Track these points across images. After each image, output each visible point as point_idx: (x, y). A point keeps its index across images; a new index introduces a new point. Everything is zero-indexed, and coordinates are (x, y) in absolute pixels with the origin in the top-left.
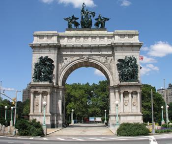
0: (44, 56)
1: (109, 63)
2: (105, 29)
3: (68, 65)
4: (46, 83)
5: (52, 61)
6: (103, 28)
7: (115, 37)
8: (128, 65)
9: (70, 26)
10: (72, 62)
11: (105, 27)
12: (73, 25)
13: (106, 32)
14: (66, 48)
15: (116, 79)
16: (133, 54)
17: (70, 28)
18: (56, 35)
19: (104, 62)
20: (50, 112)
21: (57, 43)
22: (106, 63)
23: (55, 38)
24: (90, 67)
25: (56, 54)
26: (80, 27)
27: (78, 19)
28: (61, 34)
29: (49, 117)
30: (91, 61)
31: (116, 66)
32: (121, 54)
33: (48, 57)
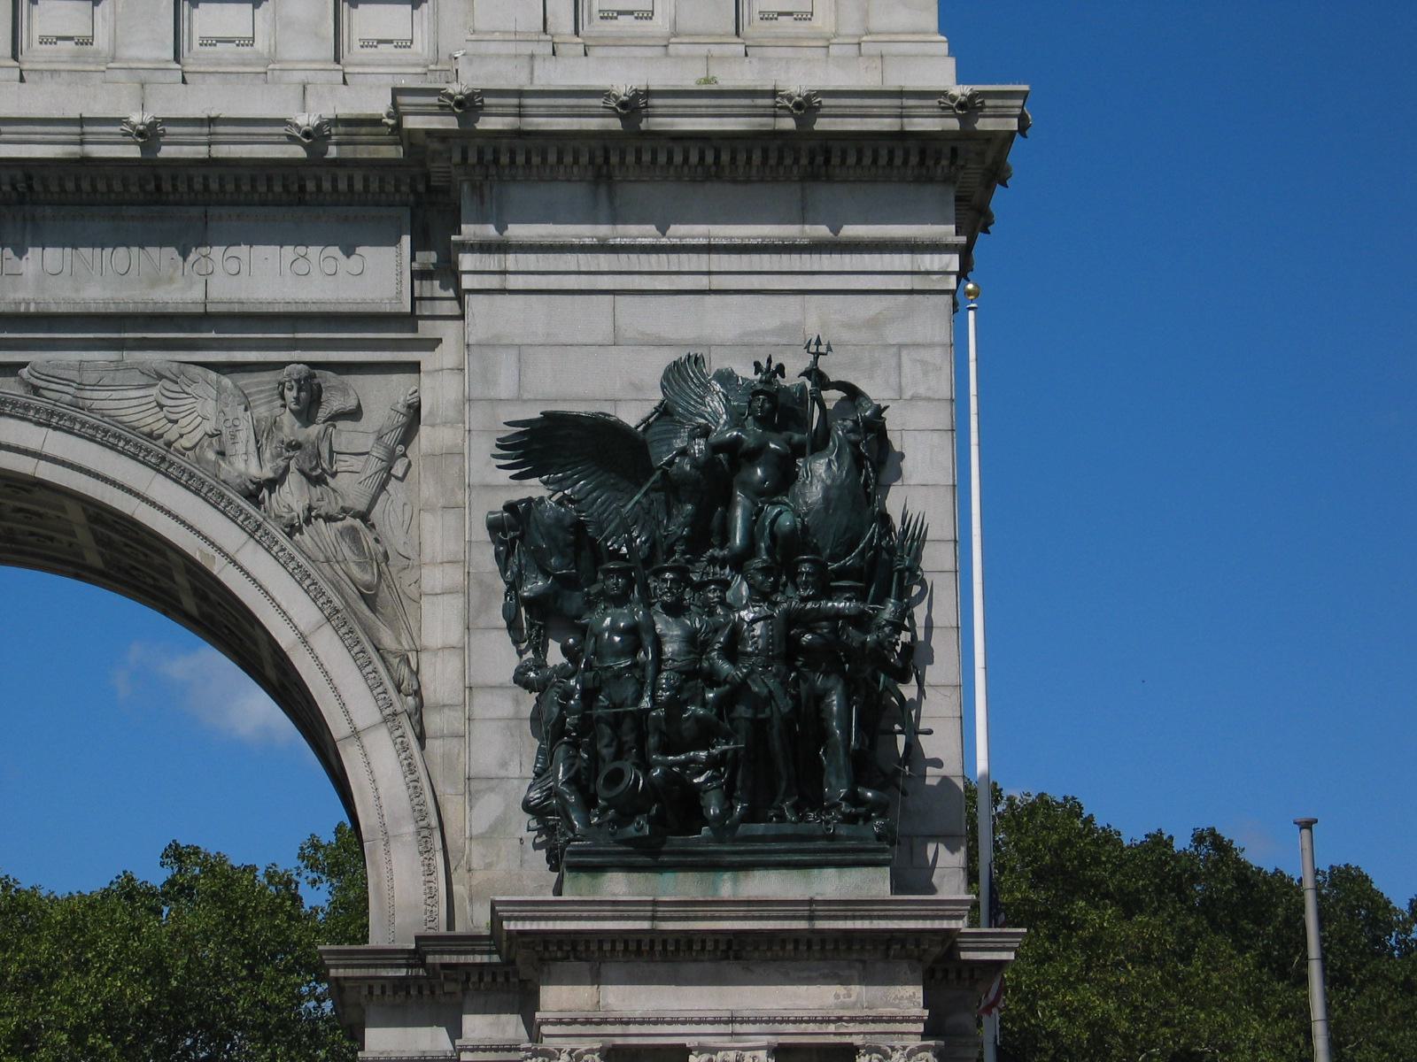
1: (351, 485)
8: (706, 532)
15: (491, 807)
16: (815, 317)
19: (247, 465)
22: (292, 496)
31: (485, 558)
32: (591, 318)
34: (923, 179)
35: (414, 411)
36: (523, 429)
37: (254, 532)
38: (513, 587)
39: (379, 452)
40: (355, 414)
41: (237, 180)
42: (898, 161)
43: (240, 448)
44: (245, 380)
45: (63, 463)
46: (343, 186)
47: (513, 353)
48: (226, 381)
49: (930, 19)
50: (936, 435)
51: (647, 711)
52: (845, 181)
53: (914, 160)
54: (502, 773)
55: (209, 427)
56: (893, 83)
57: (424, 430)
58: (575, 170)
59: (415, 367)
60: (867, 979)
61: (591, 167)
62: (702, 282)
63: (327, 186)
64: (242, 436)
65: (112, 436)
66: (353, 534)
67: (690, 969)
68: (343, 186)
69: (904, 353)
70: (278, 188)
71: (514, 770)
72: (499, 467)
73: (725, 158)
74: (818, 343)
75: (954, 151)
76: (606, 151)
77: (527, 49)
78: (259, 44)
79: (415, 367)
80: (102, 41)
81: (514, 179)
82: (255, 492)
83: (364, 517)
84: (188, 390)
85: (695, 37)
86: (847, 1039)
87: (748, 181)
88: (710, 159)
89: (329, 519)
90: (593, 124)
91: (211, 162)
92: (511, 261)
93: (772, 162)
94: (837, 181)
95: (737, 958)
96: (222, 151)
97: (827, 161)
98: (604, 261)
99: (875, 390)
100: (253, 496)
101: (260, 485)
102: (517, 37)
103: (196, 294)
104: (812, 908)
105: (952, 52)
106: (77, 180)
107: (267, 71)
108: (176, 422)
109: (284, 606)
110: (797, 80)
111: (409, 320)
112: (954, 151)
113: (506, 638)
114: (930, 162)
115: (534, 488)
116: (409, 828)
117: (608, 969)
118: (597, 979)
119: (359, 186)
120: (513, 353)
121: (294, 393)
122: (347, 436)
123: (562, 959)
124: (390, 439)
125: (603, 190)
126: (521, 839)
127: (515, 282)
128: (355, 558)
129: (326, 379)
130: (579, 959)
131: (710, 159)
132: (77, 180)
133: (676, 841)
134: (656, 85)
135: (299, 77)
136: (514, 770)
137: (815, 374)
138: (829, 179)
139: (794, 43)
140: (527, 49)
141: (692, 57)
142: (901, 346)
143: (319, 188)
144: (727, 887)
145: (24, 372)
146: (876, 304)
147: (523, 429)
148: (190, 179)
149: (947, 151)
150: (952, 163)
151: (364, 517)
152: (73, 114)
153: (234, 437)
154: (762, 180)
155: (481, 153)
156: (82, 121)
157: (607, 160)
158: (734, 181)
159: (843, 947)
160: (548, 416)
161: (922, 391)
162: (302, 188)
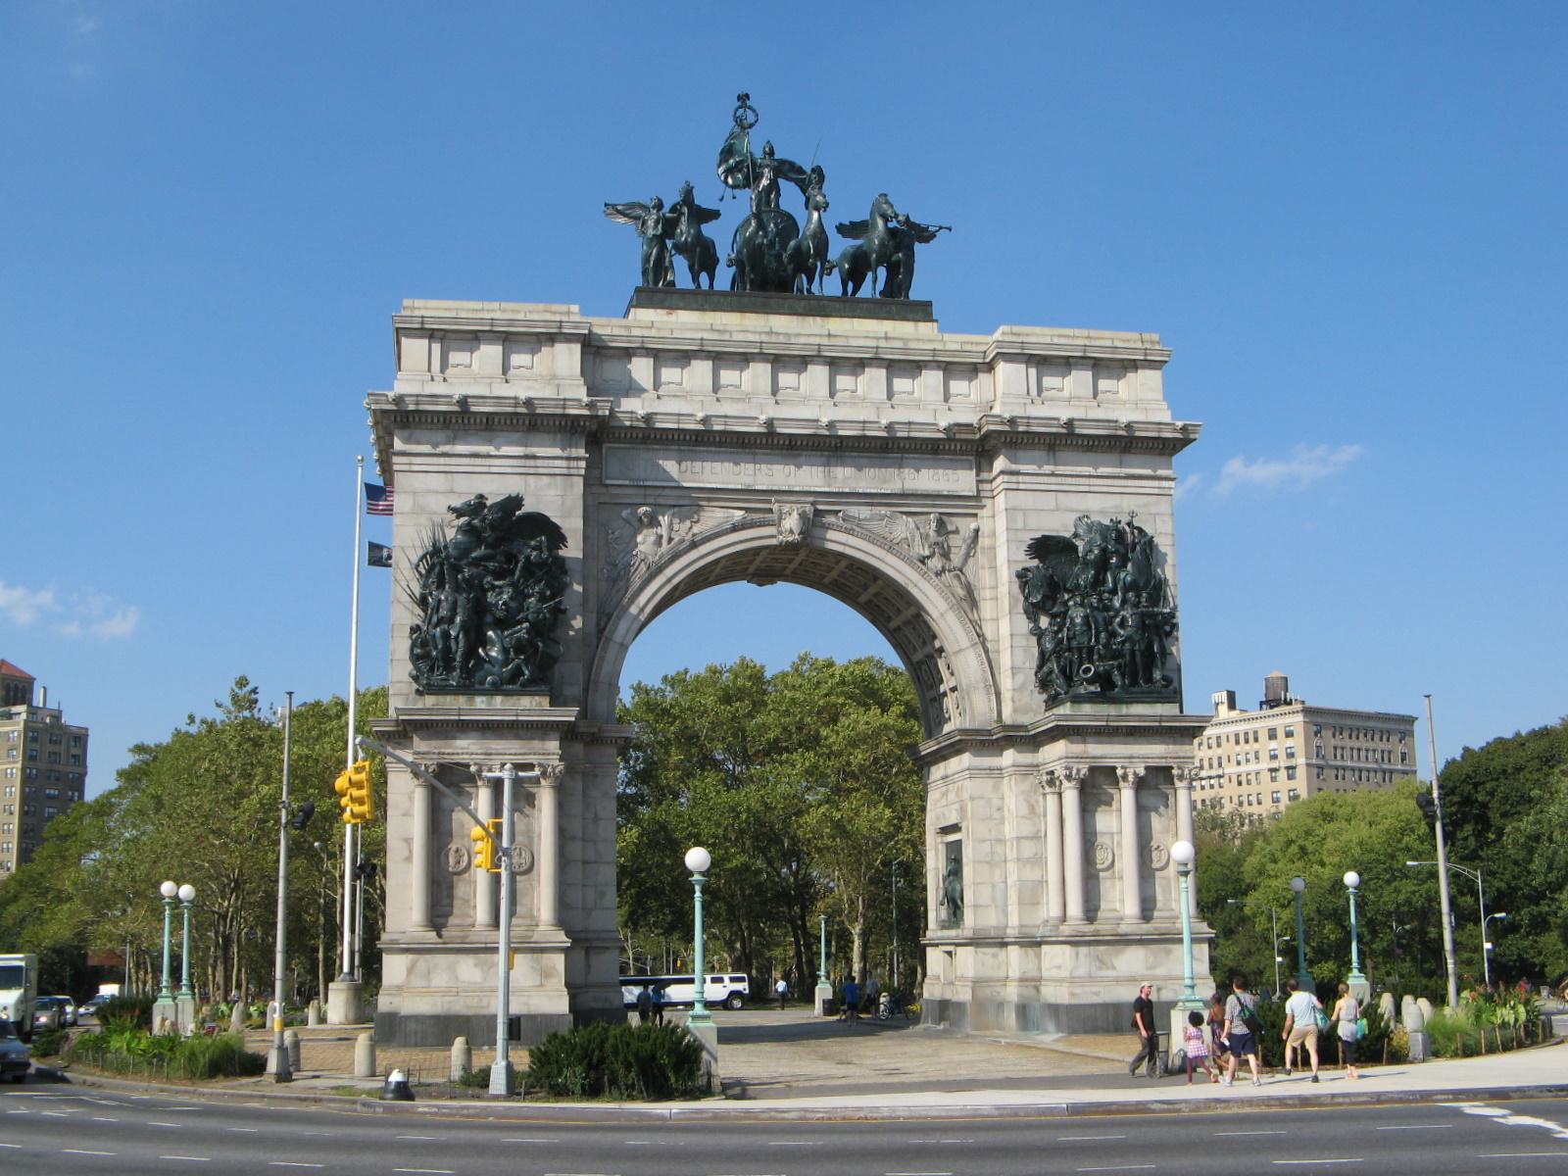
0: (495, 490)
1: (956, 559)
2: (922, 311)
3: (660, 569)
4: (526, 701)
5: (556, 536)
6: (897, 301)
7: (1002, 368)
9: (657, 269)
10: (694, 545)
11: (915, 294)
12: (681, 273)
13: (926, 329)
14: (651, 437)
17: (656, 290)
18: (569, 338)
20: (562, 921)
21: (582, 394)
22: (936, 563)
23: (567, 359)
24: (780, 585)
25: (579, 483)
26: (724, 277)
27: (714, 215)
28: (606, 328)
29: (559, 961)
30: (837, 540)
33: (515, 502)
35: (977, 531)
37: (923, 575)
38: (1026, 599)
39: (964, 547)
40: (957, 532)
43: (916, 543)
44: (918, 519)
45: (854, 548)
47: (1021, 513)
48: (910, 519)
49: (1160, 396)
51: (1093, 647)
55: (903, 536)
56: (1157, 420)
57: (980, 539)
59: (976, 515)
60: (1175, 743)
62: (1087, 489)
65: (873, 538)
66: (958, 576)
67: (1116, 739)
71: (1027, 665)
77: (1023, 401)
78: (916, 395)
79: (976, 515)
80: (860, 392)
82: (923, 560)
83: (961, 570)
85: (1079, 398)
89: (950, 571)
90: (1054, 430)
91: (909, 438)
92: (1021, 478)
96: (913, 434)
98: (1053, 480)
99: (1149, 530)
100: (923, 562)
101: (924, 558)
102: (1019, 396)
104: (1161, 718)
105: (1169, 408)
107: (918, 405)
110: (1124, 417)
111: (978, 497)
113: (1025, 617)
115: (1035, 562)
117: (1089, 739)
118: (1084, 742)
120: (1021, 513)
122: (954, 540)
124: (969, 541)
125: (1051, 454)
127: (1022, 486)
129: (945, 518)
133: (1107, 693)
134: (1076, 416)
135: (933, 407)
136: (1027, 665)
137: (1129, 524)
138: (1129, 452)
139: (1114, 402)
140: (1023, 401)
141: (1079, 406)
144: (1124, 710)
145: (841, 514)
151: (961, 570)
152: (861, 419)
156: (864, 422)
160: (1044, 537)
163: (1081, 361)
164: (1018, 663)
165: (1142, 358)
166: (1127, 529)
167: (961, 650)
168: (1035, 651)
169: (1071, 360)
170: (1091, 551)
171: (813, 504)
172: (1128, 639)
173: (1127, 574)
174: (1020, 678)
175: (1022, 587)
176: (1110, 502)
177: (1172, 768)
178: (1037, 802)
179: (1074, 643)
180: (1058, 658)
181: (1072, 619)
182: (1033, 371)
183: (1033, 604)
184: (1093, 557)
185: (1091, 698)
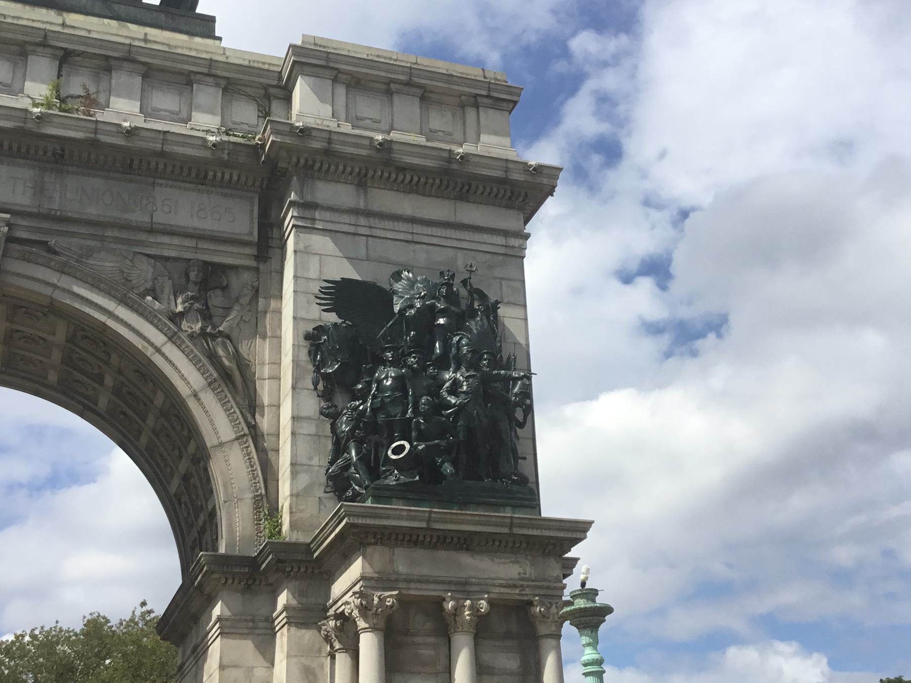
34: (508, 207)
36: (332, 285)
37: (172, 338)
38: (317, 369)
41: (174, 166)
42: (500, 196)
46: (227, 177)
47: (317, 258)
50: (519, 320)
51: (411, 419)
52: (474, 202)
53: (509, 194)
54: (309, 463)
55: (149, 285)
58: (350, 177)
61: (357, 178)
63: (219, 175)
64: (167, 290)
68: (227, 177)
69: (503, 282)
70: (193, 175)
71: (315, 461)
72: (317, 304)
73: (423, 180)
74: (471, 266)
75: (526, 194)
76: (367, 170)
81: (319, 179)
84: (137, 266)
86: (525, 598)
87: (429, 196)
88: (416, 179)
93: (443, 187)
94: (471, 202)
95: (467, 549)
97: (468, 191)
103: (147, 219)
106: (89, 154)
108: (131, 281)
109: (186, 375)
112: (526, 194)
114: (513, 199)
115: (332, 318)
116: (248, 496)
119: (235, 178)
121: (196, 273)
123: (376, 544)
126: (319, 498)
128: (225, 355)
130: (381, 544)
131: (416, 179)
132: (89, 154)
136: (315, 461)
137: (464, 282)
142: (503, 279)
143: (215, 176)
146: (488, 256)
147: (332, 285)
148: (149, 163)
149: (523, 194)
150: (523, 200)
153: (162, 291)
154: (437, 197)
155: (306, 161)
157: (366, 175)
158: (424, 195)
159: (524, 545)
161: (512, 299)
162: (206, 177)
163: (406, 89)
164: (302, 459)
165: (484, 93)
166: (463, 292)
167: (221, 445)
168: (329, 445)
169: (392, 86)
170: (411, 306)
171: (9, 225)
172: (461, 408)
173: (463, 342)
174: (304, 479)
175: (312, 354)
176: (440, 256)
177: (530, 603)
178: (322, 667)
179: (381, 417)
180: (359, 443)
181: (379, 382)
182: (341, 91)
183: (326, 377)
184: (413, 312)
185: (405, 493)
